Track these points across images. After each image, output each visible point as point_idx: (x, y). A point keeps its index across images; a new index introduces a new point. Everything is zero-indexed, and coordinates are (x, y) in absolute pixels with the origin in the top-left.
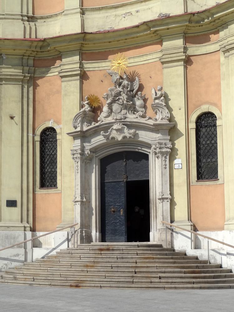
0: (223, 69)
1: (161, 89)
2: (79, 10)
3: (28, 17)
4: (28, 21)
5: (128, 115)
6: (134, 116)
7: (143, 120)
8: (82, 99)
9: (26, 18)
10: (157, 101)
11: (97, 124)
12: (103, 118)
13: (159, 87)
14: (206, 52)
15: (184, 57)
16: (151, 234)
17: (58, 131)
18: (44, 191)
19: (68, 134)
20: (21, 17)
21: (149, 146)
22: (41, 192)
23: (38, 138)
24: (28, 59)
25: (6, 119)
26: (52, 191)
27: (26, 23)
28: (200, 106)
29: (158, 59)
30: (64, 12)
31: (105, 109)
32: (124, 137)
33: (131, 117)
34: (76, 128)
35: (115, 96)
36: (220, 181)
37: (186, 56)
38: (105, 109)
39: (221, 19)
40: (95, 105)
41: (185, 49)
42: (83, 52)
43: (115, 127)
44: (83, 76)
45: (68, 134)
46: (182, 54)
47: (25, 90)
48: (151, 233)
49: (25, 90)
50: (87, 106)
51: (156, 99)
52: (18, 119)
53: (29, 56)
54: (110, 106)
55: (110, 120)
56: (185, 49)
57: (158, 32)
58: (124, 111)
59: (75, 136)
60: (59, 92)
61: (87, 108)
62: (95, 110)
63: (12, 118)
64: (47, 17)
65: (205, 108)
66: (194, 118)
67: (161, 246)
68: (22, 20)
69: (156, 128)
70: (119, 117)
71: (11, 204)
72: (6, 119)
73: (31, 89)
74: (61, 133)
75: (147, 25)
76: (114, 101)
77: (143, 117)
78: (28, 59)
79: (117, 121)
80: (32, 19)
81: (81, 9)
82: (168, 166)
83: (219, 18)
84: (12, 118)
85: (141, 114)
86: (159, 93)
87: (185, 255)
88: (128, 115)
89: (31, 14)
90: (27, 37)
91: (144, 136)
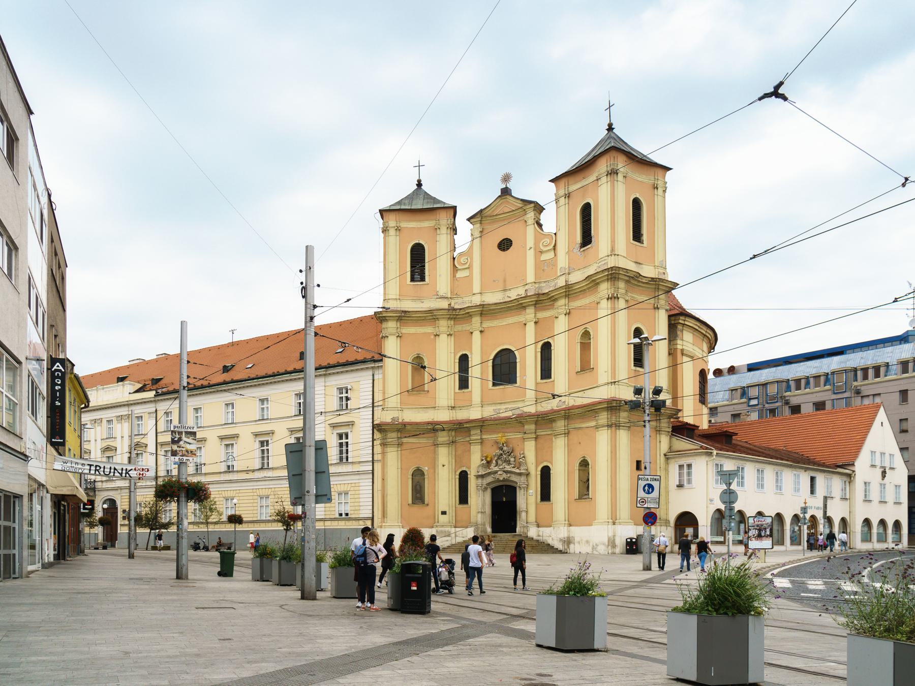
0: (554, 444)
1: (523, 454)
2: (480, 405)
3: (451, 407)
5: (506, 466)
6: (509, 467)
7: (514, 470)
8: (482, 456)
10: (521, 460)
11: (490, 471)
12: (493, 468)
13: (522, 452)
16: (517, 529)
17: (469, 473)
18: (461, 506)
19: (475, 476)
21: (517, 483)
23: (458, 477)
25: (440, 466)
26: (465, 506)
27: (451, 411)
28: (543, 462)
31: (494, 462)
32: (504, 478)
33: (508, 468)
34: (478, 472)
35: (499, 456)
36: (551, 502)
38: (494, 462)
40: (488, 459)
43: (499, 473)
44: (482, 442)
45: (475, 476)
47: (450, 450)
48: (517, 529)
50: (484, 460)
51: (520, 459)
54: (496, 461)
55: (496, 469)
58: (504, 464)
59: (478, 477)
60: (469, 451)
61: (484, 462)
62: (489, 463)
65: (545, 464)
66: (539, 468)
67: (521, 535)
69: (520, 474)
70: (501, 467)
71: (444, 513)
74: (470, 474)
76: (498, 458)
77: (513, 467)
79: (501, 469)
82: (525, 495)
83: (552, 418)
84: (443, 466)
85: (513, 466)
86: (522, 456)
87: (533, 539)
88: (506, 466)
91: (514, 478)
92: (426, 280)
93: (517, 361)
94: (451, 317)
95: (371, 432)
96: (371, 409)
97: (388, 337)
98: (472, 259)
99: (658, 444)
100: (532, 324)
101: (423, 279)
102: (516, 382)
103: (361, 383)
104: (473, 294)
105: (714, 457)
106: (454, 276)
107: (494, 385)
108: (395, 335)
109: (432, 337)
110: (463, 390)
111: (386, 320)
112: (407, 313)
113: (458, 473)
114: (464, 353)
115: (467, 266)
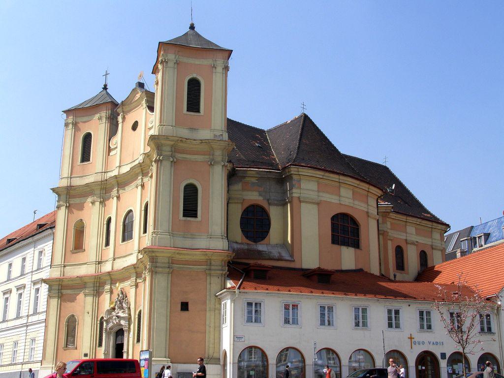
3: (99, 262)
22: (98, 349)
23: (99, 322)
25: (86, 314)
41: (136, 280)
47: (95, 299)
49: (95, 299)
52: (90, 313)
63: (88, 313)
72: (86, 314)
73: (97, 298)
84: (88, 313)
99: (208, 286)
105: (237, 296)
106: (109, 155)
109: (91, 204)
112: (73, 188)
113: (99, 319)
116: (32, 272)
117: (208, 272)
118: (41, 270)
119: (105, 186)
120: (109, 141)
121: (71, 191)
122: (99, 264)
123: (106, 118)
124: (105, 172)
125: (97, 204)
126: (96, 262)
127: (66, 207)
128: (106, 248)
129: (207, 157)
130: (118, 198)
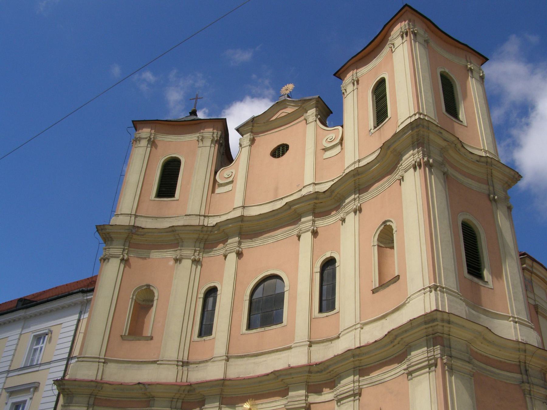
2: (225, 357)
3: (183, 362)
4: (182, 366)
9: (181, 363)
14: (325, 400)
15: (305, 405)
20: (176, 363)
24: (177, 401)
27: (180, 368)
29: (283, 406)
30: (212, 359)
37: (306, 404)
39: (335, 370)
41: (307, 396)
42: (225, 396)
46: (304, 401)
53: (178, 399)
56: (307, 396)
57: (284, 381)
64: (200, 363)
68: (177, 365)
75: (275, 374)
78: (177, 401)
80: (185, 364)
81: (227, 356)
89: (185, 359)
90: (179, 380)
92: (175, 196)
93: (286, 289)
94: (201, 236)
95: (55, 398)
96: (65, 362)
97: (109, 259)
98: (237, 171)
100: (309, 234)
101: (171, 194)
102: (282, 322)
103: (63, 325)
104: (234, 209)
106: (213, 191)
107: (250, 327)
108: (118, 257)
109: (172, 263)
110: (204, 338)
111: (111, 237)
112: (141, 230)
114: (212, 285)
115: (231, 179)
116: (8, 372)
117: (526, 387)
118: (37, 369)
119: (206, 237)
120: (216, 173)
121: (135, 237)
122: (182, 366)
123: (212, 141)
124: (205, 216)
125: (187, 263)
126: (178, 361)
127: (122, 260)
128: (199, 339)
129: (485, 187)
130: (239, 254)
